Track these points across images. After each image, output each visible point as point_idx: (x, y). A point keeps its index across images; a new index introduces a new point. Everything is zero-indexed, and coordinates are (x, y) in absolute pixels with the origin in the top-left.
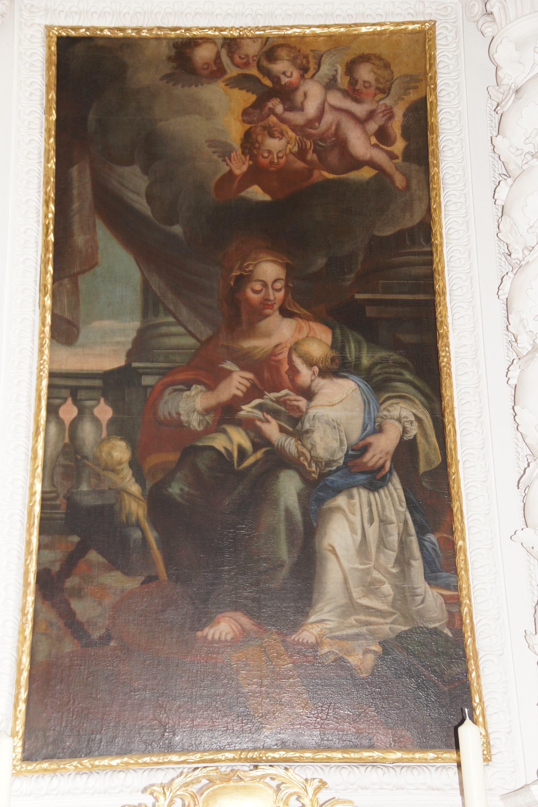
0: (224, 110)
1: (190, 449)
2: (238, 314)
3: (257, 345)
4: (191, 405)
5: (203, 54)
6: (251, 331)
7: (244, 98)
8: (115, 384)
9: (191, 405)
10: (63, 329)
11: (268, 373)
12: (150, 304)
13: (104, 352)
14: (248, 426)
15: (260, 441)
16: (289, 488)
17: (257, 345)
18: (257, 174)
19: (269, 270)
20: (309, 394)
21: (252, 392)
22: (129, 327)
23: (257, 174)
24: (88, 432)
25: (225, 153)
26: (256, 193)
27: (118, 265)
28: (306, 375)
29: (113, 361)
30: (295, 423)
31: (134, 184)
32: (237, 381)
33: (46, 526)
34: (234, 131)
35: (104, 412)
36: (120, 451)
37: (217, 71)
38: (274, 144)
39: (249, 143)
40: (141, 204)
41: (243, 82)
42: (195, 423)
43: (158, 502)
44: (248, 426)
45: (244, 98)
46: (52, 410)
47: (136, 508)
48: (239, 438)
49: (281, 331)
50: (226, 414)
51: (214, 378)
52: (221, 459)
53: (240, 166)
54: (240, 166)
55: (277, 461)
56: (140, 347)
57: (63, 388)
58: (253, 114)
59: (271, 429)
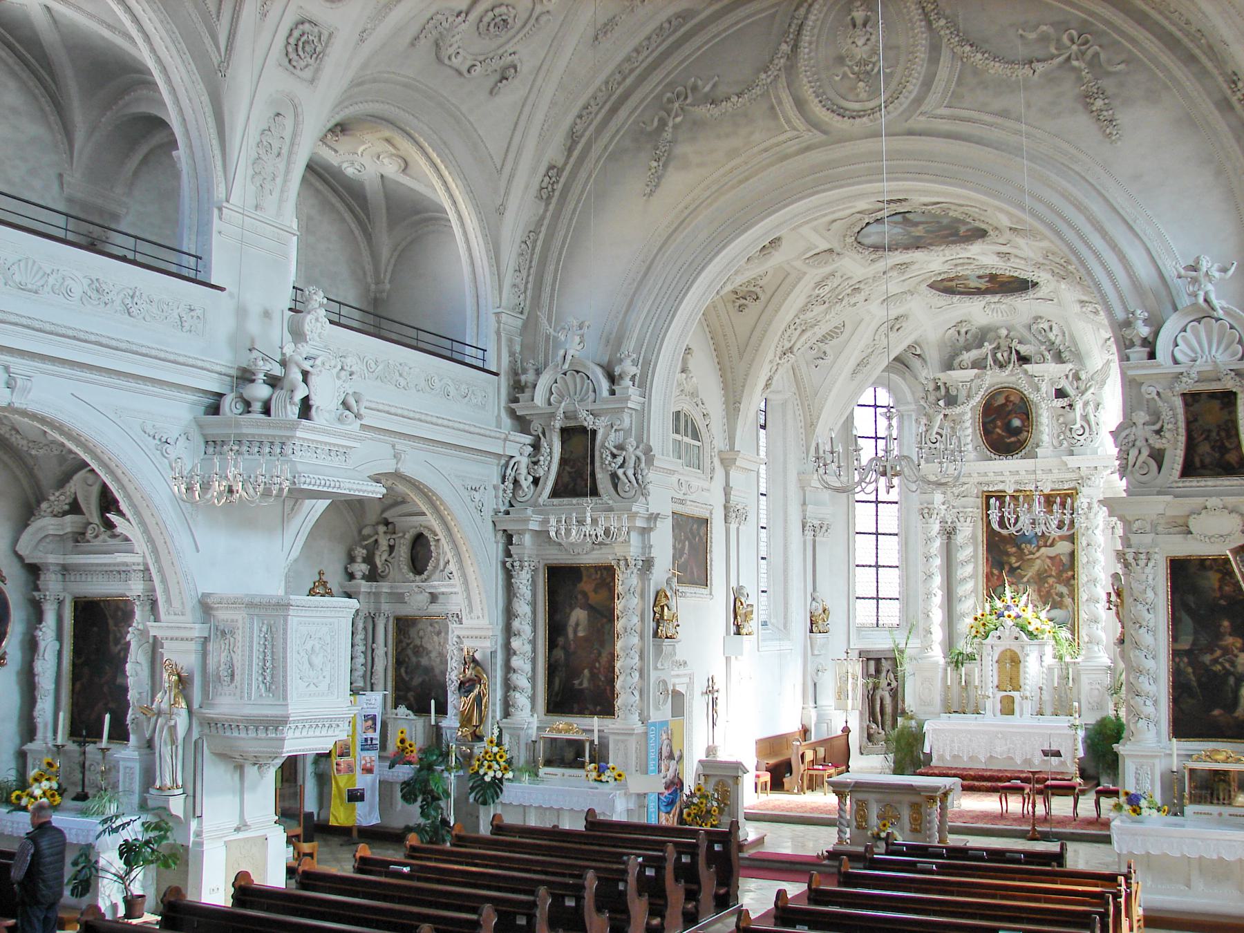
0: (1213, 579)
1: (1207, 669)
2: (1219, 636)
3: (1223, 643)
4: (1207, 658)
5: (1208, 563)
6: (1221, 640)
7: (1219, 575)
8: (1188, 653)
9: (1207, 658)
10: (1175, 639)
11: (1226, 651)
12: (1196, 632)
13: (1185, 645)
14: (1221, 664)
15: (1224, 668)
16: (1232, 680)
17: (1223, 643)
18: (1222, 597)
19: (1226, 623)
20: (1236, 656)
21: (1223, 655)
22: (1190, 639)
23: (1222, 597)
24: (1182, 665)
25: (1214, 590)
26: (1222, 602)
27: (1187, 621)
28: (1236, 651)
29: (1187, 647)
30: (1233, 663)
31: (1191, 600)
32: (1218, 653)
33: (1174, 688)
34: (1216, 585)
35: (1186, 660)
36: (1190, 670)
37: (1211, 568)
38: (1227, 588)
39: (1220, 588)
40: (1193, 606)
41: (1218, 571)
42: (1208, 663)
43: (1198, 681)
44: (1221, 664)
45: (1219, 575)
46: (1173, 660)
47: (1195, 684)
48: (1219, 667)
49: (1229, 640)
50: (1215, 661)
51: (1212, 652)
52: (1215, 673)
53: (1218, 595)
54: (1218, 595)
55: (1228, 673)
56: (1194, 644)
57: (1176, 653)
58: (1221, 580)
59: (1227, 665)
